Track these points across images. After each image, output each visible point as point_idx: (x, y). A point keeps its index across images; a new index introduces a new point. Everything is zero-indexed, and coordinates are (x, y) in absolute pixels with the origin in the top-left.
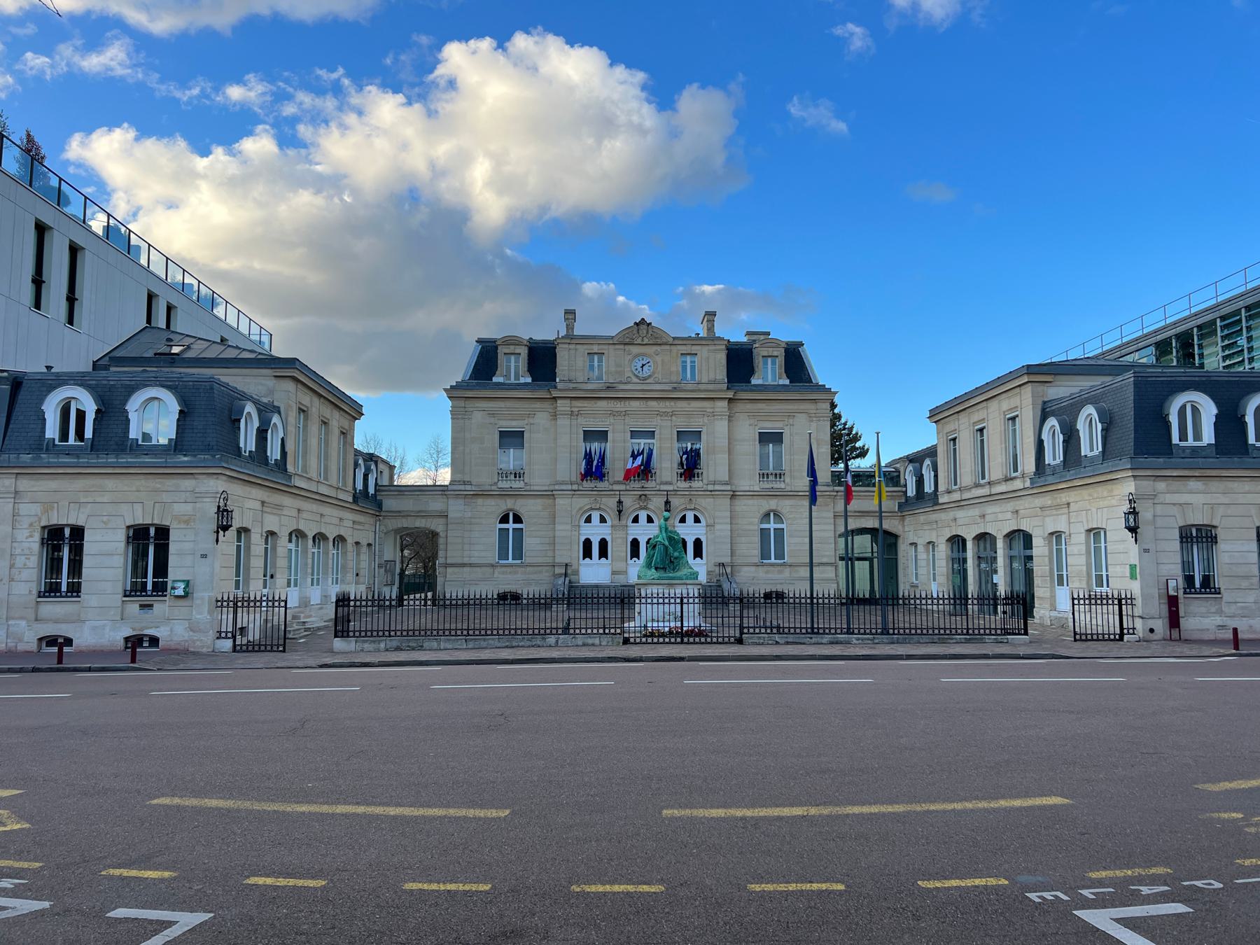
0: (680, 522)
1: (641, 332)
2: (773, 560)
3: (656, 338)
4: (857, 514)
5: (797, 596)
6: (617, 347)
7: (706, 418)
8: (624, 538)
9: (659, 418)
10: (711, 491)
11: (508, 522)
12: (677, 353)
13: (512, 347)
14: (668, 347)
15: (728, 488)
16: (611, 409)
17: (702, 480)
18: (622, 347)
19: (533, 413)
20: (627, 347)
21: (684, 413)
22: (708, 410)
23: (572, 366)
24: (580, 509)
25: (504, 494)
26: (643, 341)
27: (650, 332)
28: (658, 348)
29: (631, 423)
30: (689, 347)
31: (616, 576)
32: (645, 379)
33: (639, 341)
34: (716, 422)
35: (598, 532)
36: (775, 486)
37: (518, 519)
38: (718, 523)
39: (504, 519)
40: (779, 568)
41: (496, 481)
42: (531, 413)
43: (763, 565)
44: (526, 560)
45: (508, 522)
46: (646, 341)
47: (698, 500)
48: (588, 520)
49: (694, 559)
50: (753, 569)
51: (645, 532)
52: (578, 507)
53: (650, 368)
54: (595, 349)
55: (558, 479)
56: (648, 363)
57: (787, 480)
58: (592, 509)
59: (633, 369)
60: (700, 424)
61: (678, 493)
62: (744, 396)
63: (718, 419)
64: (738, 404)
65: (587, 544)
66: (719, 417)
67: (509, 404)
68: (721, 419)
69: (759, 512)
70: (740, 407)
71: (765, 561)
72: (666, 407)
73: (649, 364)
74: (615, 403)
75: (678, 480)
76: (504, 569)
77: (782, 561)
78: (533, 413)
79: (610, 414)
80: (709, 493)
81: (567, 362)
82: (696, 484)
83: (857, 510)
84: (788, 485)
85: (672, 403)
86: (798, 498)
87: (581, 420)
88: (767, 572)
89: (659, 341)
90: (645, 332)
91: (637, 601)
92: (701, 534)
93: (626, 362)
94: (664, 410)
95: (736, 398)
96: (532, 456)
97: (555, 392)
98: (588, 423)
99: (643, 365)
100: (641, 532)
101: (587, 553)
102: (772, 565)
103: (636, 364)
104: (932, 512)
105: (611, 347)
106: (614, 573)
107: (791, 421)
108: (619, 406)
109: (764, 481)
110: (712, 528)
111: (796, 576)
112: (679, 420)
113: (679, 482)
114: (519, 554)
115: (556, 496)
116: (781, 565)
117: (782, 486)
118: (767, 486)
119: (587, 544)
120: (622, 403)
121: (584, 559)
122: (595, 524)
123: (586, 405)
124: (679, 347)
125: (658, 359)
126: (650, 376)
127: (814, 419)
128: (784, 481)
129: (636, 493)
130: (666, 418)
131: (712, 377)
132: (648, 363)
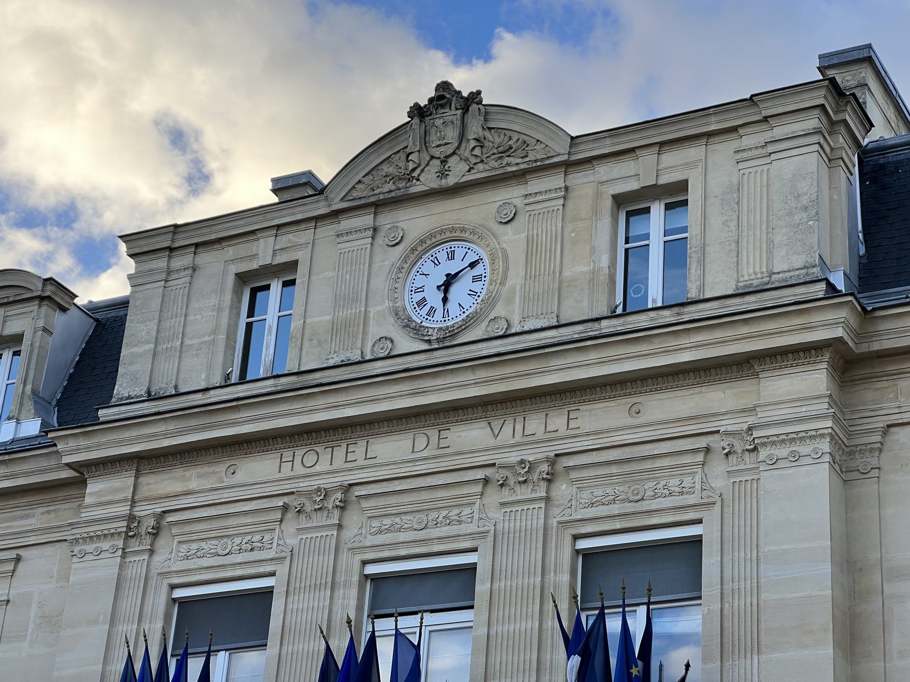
1: (434, 139)
3: (507, 151)
6: (348, 223)
7: (718, 468)
9: (494, 496)
12: (598, 195)
14: (556, 181)
16: (287, 487)
18: (365, 220)
20: (386, 219)
22: (727, 424)
26: (443, 174)
27: (475, 129)
28: (513, 194)
30: (648, 159)
33: (429, 180)
34: (769, 480)
46: (458, 172)
53: (477, 287)
56: (472, 265)
59: (409, 302)
60: (692, 500)
66: (782, 451)
68: (796, 458)
72: (530, 441)
73: (478, 270)
74: (310, 459)
79: (285, 508)
81: (153, 325)
85: (558, 421)
89: (514, 164)
90: (451, 134)
93: (380, 283)
94: (513, 457)
95: (876, 347)
97: (72, 444)
99: (450, 279)
105: (327, 231)
112: (586, 496)
120: (340, 452)
123: (193, 485)
124: (603, 171)
126: (468, 323)
130: (524, 493)
132: (472, 265)
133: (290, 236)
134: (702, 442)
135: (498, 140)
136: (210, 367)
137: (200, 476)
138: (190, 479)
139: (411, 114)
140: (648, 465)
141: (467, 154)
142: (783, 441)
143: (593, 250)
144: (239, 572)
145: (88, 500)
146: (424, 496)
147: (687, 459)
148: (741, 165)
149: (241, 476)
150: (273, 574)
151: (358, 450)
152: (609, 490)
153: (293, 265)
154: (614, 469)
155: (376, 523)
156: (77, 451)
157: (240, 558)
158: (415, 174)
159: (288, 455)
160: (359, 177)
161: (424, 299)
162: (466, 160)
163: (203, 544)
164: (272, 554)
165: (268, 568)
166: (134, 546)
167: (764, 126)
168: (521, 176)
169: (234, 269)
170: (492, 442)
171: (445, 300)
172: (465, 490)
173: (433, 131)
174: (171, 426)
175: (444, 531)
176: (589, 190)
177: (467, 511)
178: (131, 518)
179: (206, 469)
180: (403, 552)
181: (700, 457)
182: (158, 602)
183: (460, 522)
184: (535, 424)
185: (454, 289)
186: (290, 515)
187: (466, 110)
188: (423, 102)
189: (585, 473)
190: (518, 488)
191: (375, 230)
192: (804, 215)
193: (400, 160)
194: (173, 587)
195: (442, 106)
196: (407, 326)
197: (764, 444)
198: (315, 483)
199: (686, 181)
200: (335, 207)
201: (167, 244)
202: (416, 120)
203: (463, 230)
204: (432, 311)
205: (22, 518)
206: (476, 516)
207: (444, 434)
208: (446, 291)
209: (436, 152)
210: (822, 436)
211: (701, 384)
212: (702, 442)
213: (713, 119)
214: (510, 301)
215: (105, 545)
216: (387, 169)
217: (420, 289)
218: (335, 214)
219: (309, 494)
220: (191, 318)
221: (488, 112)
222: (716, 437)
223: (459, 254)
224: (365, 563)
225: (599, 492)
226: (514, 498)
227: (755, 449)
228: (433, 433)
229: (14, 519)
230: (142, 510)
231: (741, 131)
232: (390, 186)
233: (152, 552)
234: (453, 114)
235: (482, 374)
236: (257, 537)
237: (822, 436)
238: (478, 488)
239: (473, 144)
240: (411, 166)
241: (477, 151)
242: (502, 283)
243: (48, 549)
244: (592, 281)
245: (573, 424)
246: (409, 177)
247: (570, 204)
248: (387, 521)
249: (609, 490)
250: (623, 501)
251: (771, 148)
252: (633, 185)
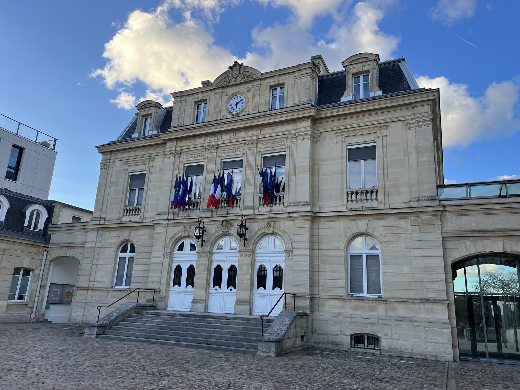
1: (234, 73)
2: (365, 294)
3: (248, 76)
4: (477, 234)
6: (217, 91)
8: (206, 264)
9: (246, 147)
10: (289, 213)
12: (267, 86)
13: (147, 109)
14: (258, 83)
15: (308, 208)
16: (206, 145)
17: (283, 203)
18: (220, 90)
19: (153, 157)
23: (182, 115)
24: (173, 236)
25: (122, 227)
26: (236, 81)
27: (242, 71)
28: (250, 85)
29: (222, 155)
30: (277, 78)
31: (195, 305)
32: (238, 114)
33: (233, 82)
34: (299, 143)
35: (188, 259)
36: (367, 205)
38: (297, 248)
40: (370, 304)
41: (121, 216)
42: (151, 157)
43: (350, 298)
46: (239, 81)
47: (277, 223)
48: (181, 248)
49: (273, 289)
50: (339, 303)
51: (228, 258)
52: (171, 235)
53: (243, 105)
55: (159, 210)
56: (242, 100)
57: (380, 197)
58: (184, 237)
59: (229, 107)
60: (284, 147)
61: (257, 217)
62: (327, 113)
63: (300, 140)
64: (325, 124)
66: (301, 137)
67: (138, 153)
68: (304, 139)
69: (346, 236)
70: (326, 126)
71: (355, 295)
72: (253, 136)
73: (243, 101)
74: (211, 139)
75: (260, 205)
77: (377, 295)
78: (153, 157)
79: (206, 149)
80: (287, 215)
81: (178, 112)
82: (277, 208)
83: (477, 228)
84: (381, 203)
85: (259, 132)
86: (393, 217)
87: (183, 158)
88: (356, 308)
89: (250, 79)
90: (237, 72)
92: (280, 261)
93: (224, 103)
94: (250, 139)
95: (320, 117)
96: (148, 193)
97: (163, 136)
99: (237, 103)
100: (224, 259)
102: (362, 299)
103: (231, 103)
105: (213, 93)
106: (194, 301)
107: (383, 132)
108: (213, 141)
109: (352, 201)
110: (291, 254)
111: (392, 314)
112: (264, 146)
113: (261, 206)
115: (155, 226)
116: (374, 300)
117: (375, 204)
118: (356, 205)
120: (216, 138)
122: (186, 252)
123: (187, 144)
124: (268, 80)
125: (250, 95)
127: (412, 126)
128: (377, 199)
129: (219, 219)
130: (252, 146)
131: (297, 102)
132: (242, 100)
133: (205, 94)
134: (286, 136)
135: (247, 74)
136: (190, 120)
137: (189, 142)
138: (187, 143)
139: (229, 68)
140: (276, 140)
141: (240, 77)
142: (301, 136)
143: (265, 97)
144: (197, 161)
145: (167, 147)
146: (233, 146)
147: (283, 139)
148: (295, 80)
149: (197, 142)
150: (204, 162)
151: (220, 138)
152: (268, 145)
153: (206, 100)
154: (269, 141)
155: (224, 152)
156: (164, 137)
157: (197, 158)
158: (230, 81)
159: (206, 138)
160: (219, 81)
161: (232, 107)
162: (240, 78)
163: (190, 156)
164: (203, 158)
165: (203, 160)
166: (177, 156)
167: (300, 71)
168: (251, 82)
169: (194, 100)
170: (246, 136)
171: (236, 107)
172: (241, 145)
173: (234, 72)
174: (183, 132)
176: (265, 85)
177: (241, 149)
178: (176, 150)
179: (190, 141)
180: (229, 157)
181: (286, 139)
182: (182, 167)
183: (240, 151)
184: (254, 132)
185: (238, 105)
186: (207, 150)
187: (240, 67)
188: (232, 66)
189: (264, 142)
190: (251, 145)
191: (222, 93)
192: (307, 90)
193: (227, 78)
194: (185, 164)
195: (235, 66)
196: (229, 112)
197: (298, 136)
198: (212, 144)
199: (284, 83)
200: (214, 88)
201: (180, 95)
202: (230, 69)
203: (240, 93)
204: (234, 109)
205: (154, 150)
206: (243, 150)
207: (236, 134)
208: (237, 105)
209: (234, 76)
210: (309, 134)
211: (286, 124)
212: (286, 136)
213: (290, 70)
214: (249, 107)
215: (171, 156)
216: (224, 80)
217: (231, 105)
218: (214, 89)
219: (210, 146)
220: (186, 110)
221: (245, 68)
222: (289, 135)
223: (239, 98)
224: (222, 159)
225: (266, 146)
226: (250, 147)
227: (296, 137)
228: (234, 134)
229: (153, 150)
230: (178, 149)
231: (295, 72)
232: (225, 83)
233: (180, 157)
234: (237, 68)
235: (244, 122)
236: (201, 154)
237: (309, 134)
238: (243, 145)
239: (242, 75)
240: (229, 79)
241: (242, 76)
242: (248, 104)
243: (160, 156)
244: (265, 103)
245: (261, 132)
246: (229, 82)
247: (261, 87)
248: (226, 151)
249: (268, 145)
250: (271, 147)
251: (301, 76)
252: (274, 84)
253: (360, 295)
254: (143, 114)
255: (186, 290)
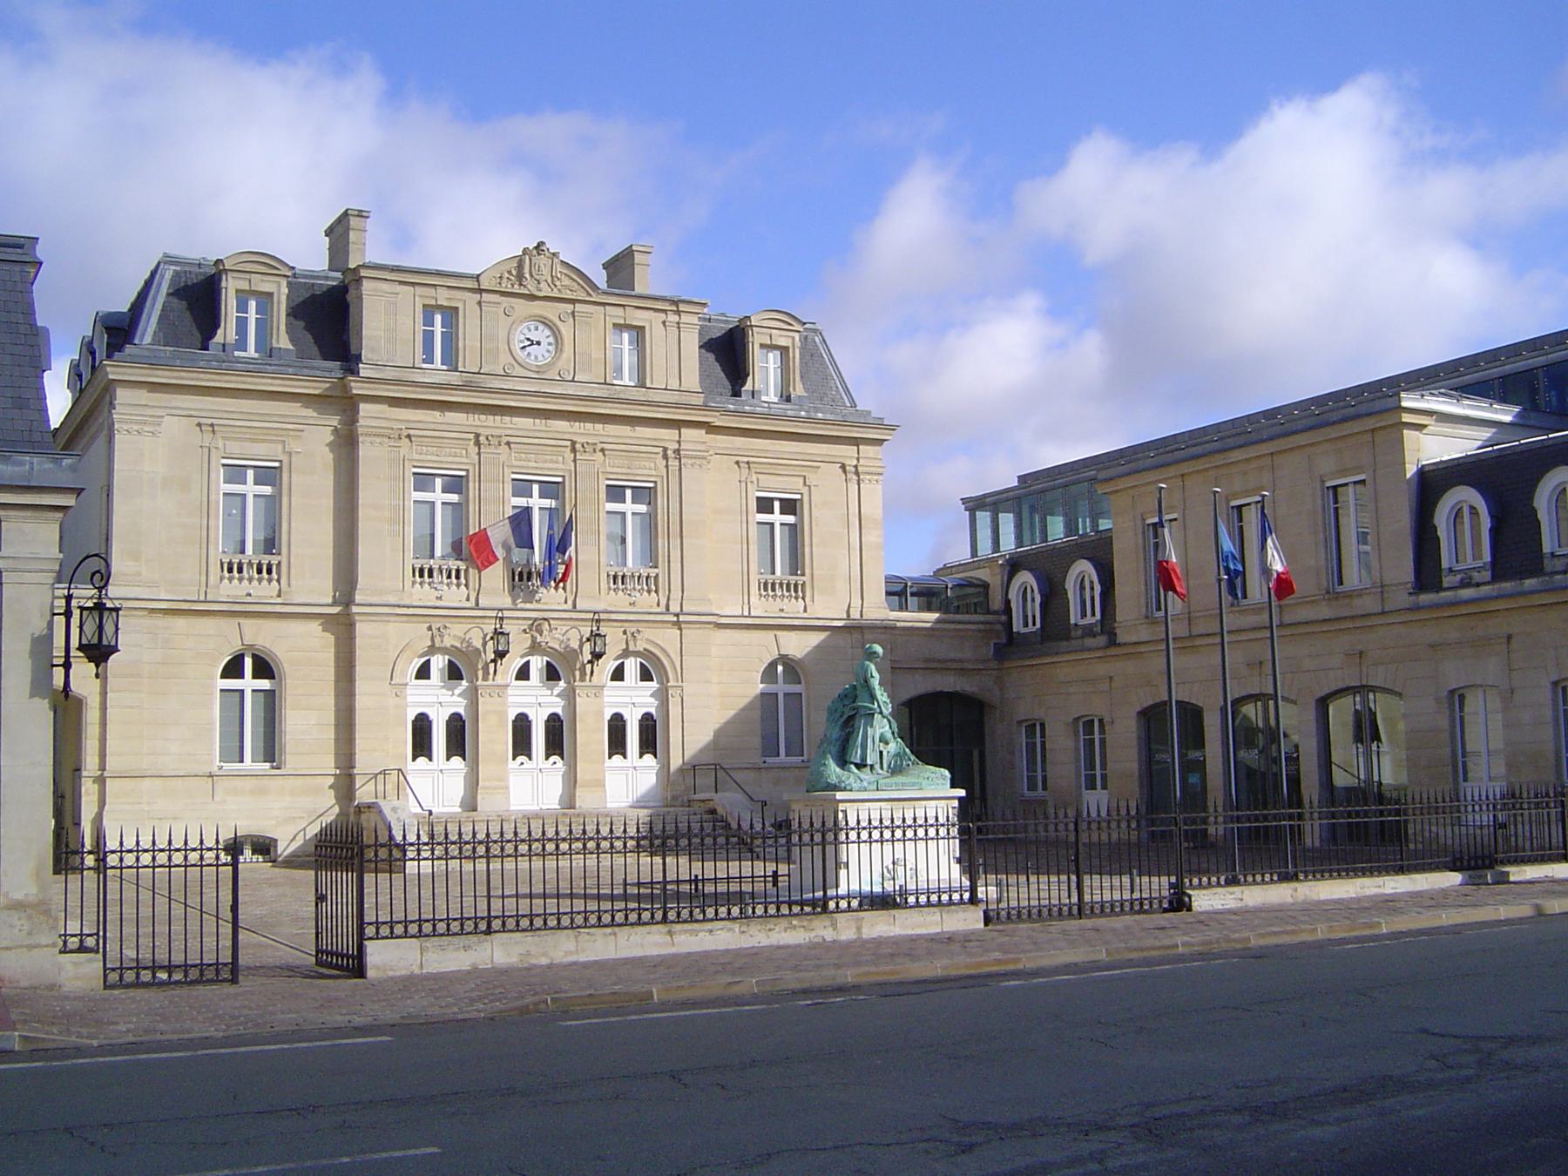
0: (613, 679)
5: (591, 833)
11: (241, 676)
21: (622, 447)
29: (515, 463)
37: (264, 668)
39: (233, 669)
44: (291, 762)
45: (241, 676)
48: (423, 672)
54: (443, 297)
60: (654, 473)
65: (422, 727)
76: (238, 782)
85: (599, 426)
91: (853, 835)
98: (423, 457)
101: (422, 745)
104: (1096, 660)
114: (271, 751)
119: (422, 727)
121: (414, 760)
157: (450, 459)
175: (550, 465)
215: (378, 440)
253: (776, 760)
254: (238, 287)
255: (447, 767)
